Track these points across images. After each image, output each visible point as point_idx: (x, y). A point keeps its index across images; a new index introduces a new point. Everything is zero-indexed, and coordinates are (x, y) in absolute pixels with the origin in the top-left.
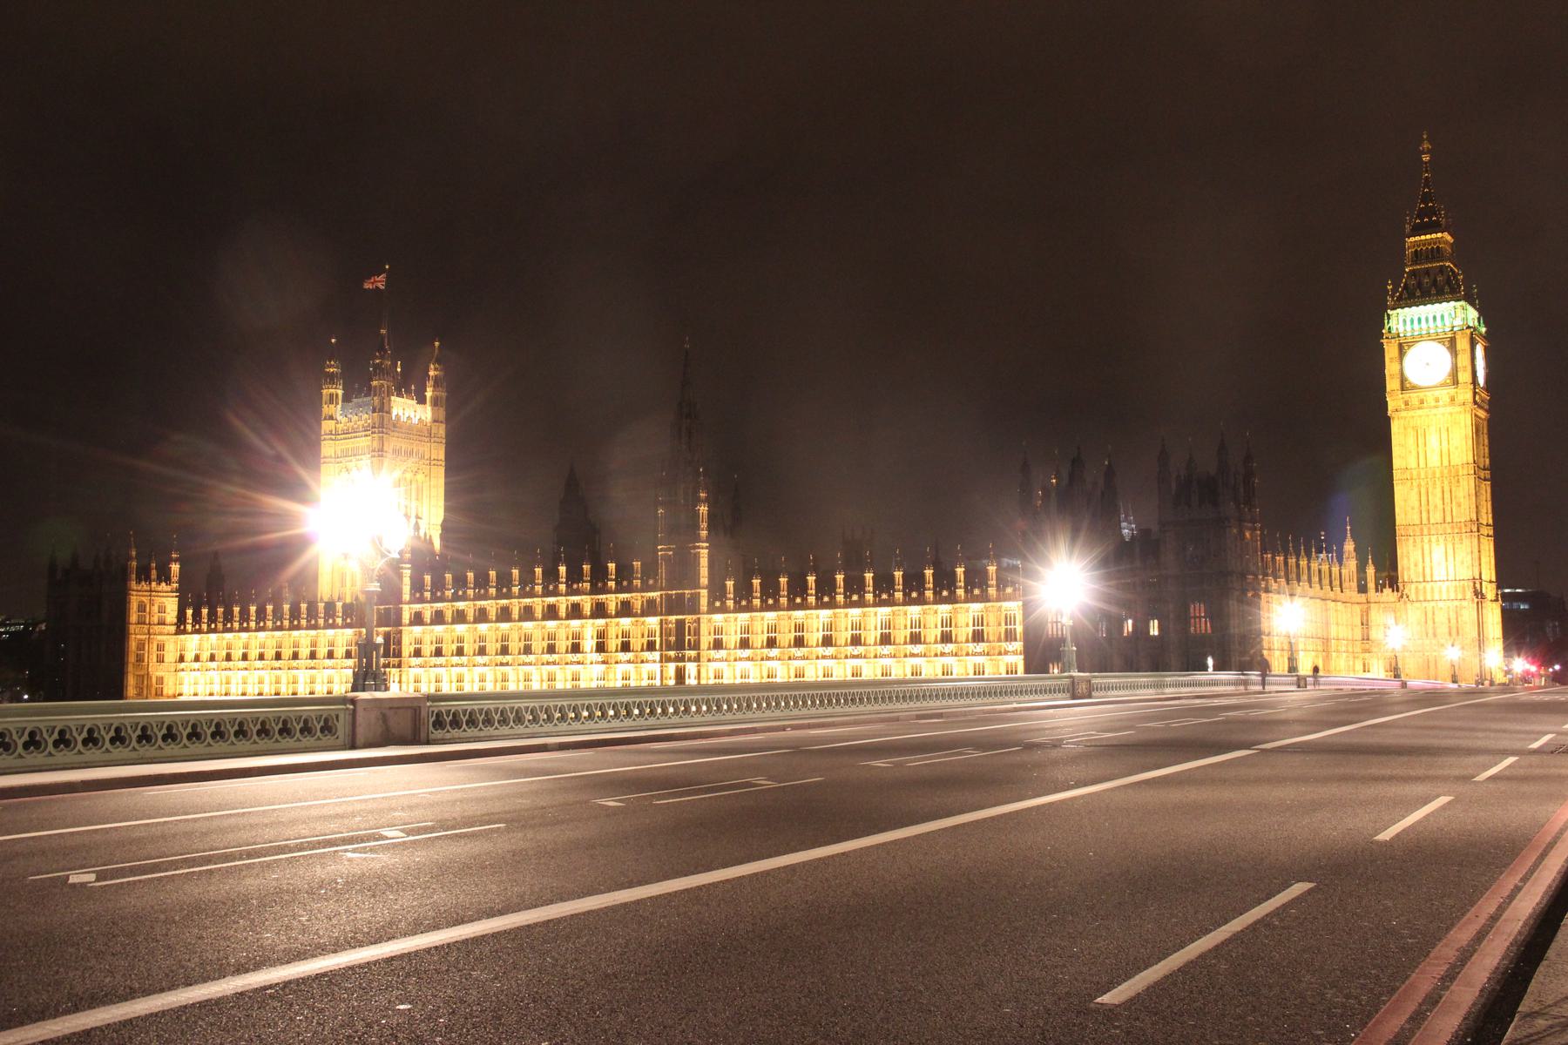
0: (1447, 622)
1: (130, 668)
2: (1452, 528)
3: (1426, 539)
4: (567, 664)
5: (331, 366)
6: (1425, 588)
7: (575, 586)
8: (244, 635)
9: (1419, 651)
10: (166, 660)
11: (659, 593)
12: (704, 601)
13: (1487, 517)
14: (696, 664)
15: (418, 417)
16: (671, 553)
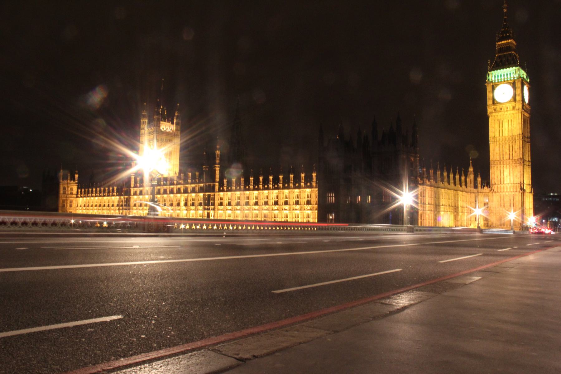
0: (509, 201)
1: (60, 208)
2: (513, 161)
3: (502, 166)
5: (144, 112)
6: (501, 186)
10: (73, 206)
12: (217, 188)
13: (528, 157)
15: (170, 129)
16: (207, 169)
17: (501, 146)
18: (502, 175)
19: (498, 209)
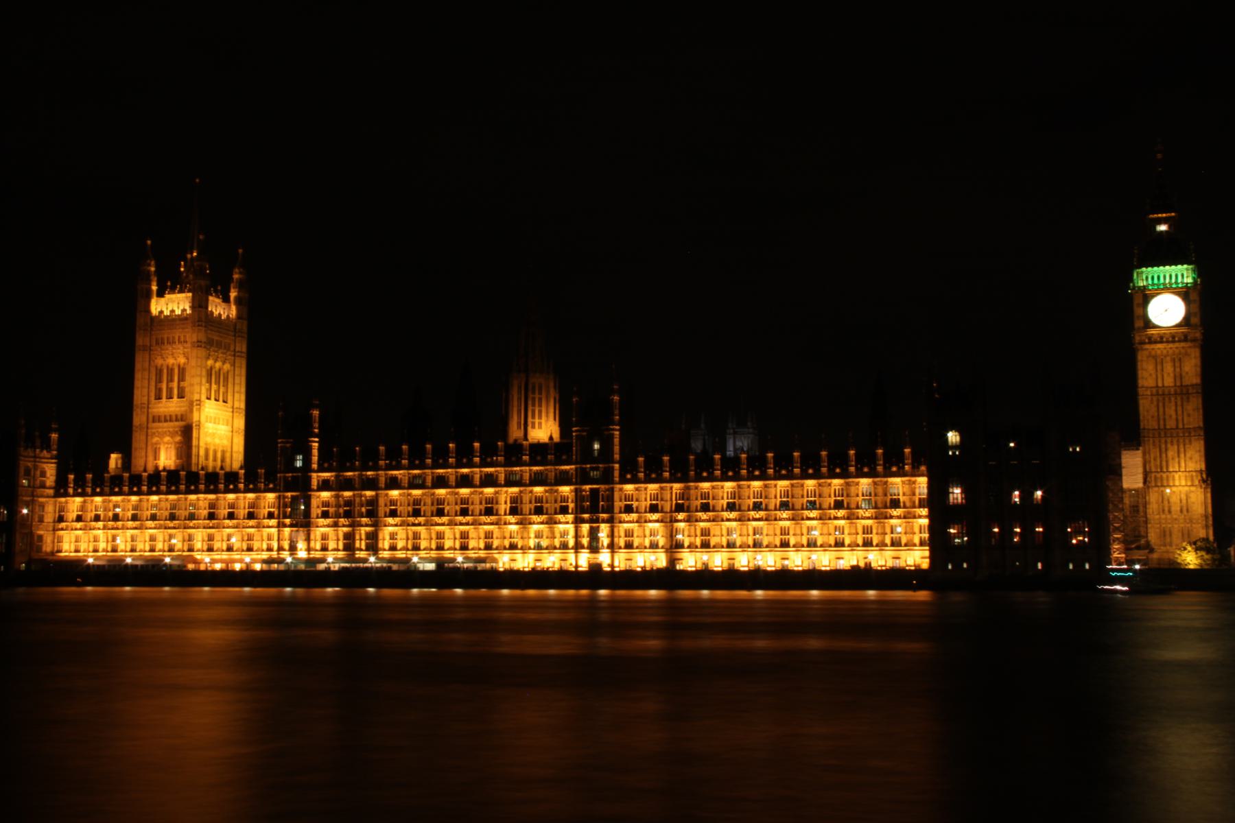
0: (1179, 502)
2: (1184, 433)
4: (480, 524)
6: (1161, 476)
7: (489, 460)
8: (134, 498)
9: (1157, 524)
10: (46, 520)
11: (573, 467)
12: (617, 473)
14: (608, 525)
15: (226, 314)
16: (585, 434)
17: (1161, 404)
18: (1164, 455)
19: (1157, 517)
